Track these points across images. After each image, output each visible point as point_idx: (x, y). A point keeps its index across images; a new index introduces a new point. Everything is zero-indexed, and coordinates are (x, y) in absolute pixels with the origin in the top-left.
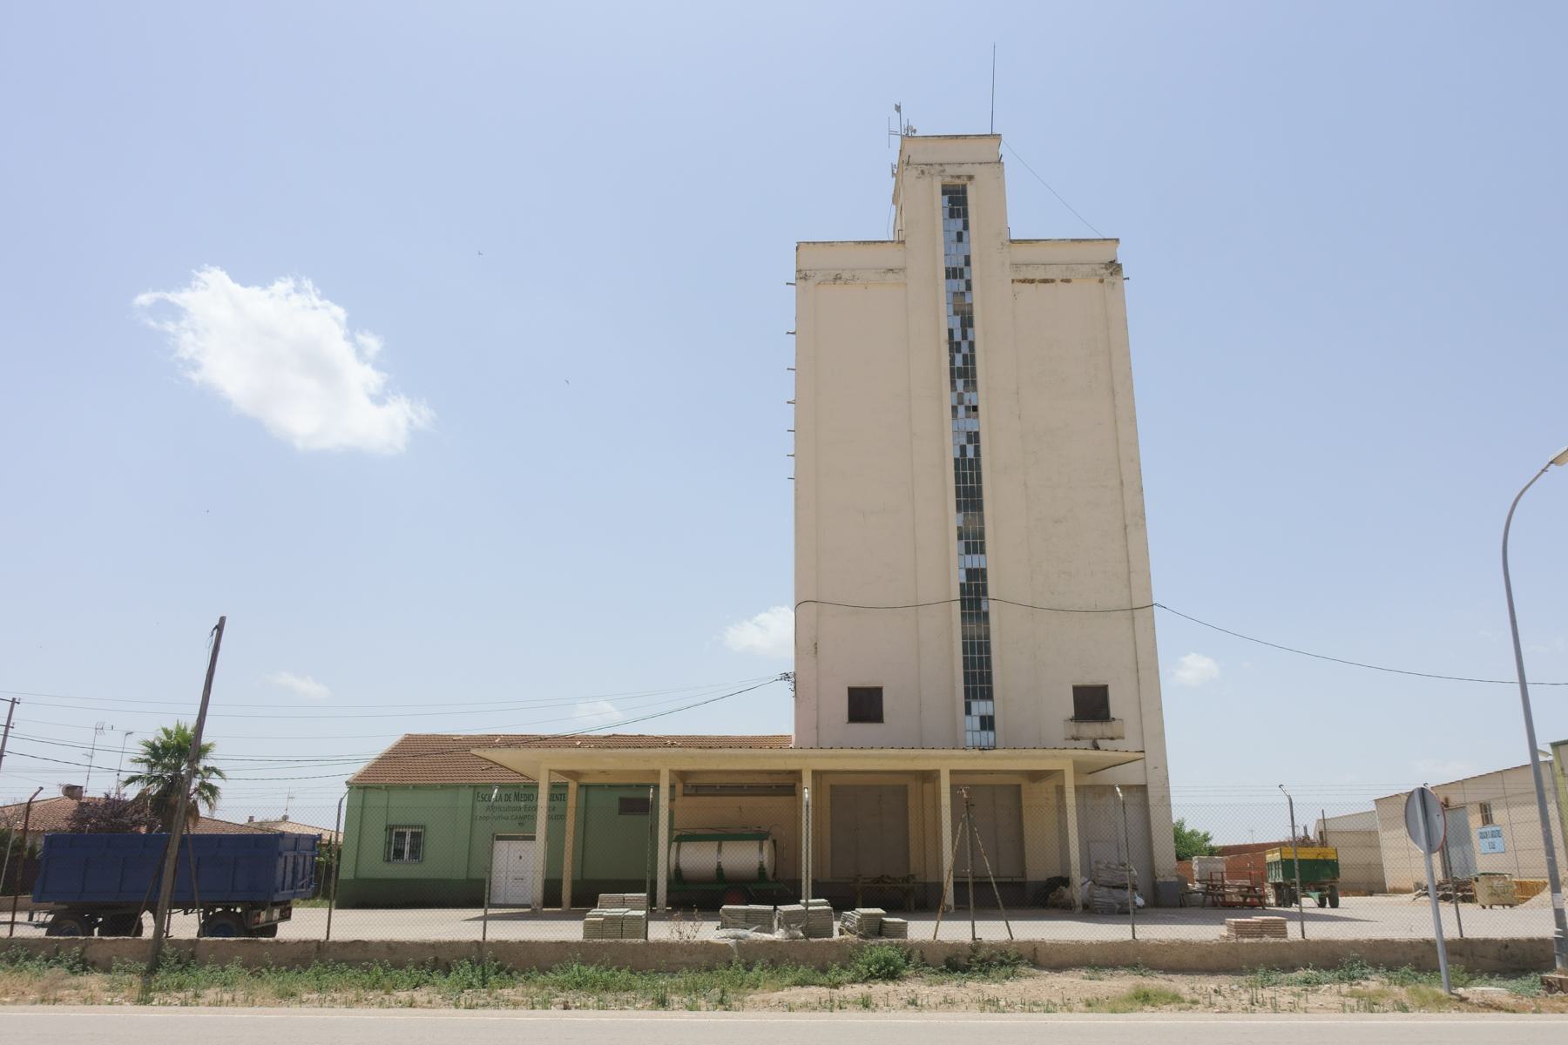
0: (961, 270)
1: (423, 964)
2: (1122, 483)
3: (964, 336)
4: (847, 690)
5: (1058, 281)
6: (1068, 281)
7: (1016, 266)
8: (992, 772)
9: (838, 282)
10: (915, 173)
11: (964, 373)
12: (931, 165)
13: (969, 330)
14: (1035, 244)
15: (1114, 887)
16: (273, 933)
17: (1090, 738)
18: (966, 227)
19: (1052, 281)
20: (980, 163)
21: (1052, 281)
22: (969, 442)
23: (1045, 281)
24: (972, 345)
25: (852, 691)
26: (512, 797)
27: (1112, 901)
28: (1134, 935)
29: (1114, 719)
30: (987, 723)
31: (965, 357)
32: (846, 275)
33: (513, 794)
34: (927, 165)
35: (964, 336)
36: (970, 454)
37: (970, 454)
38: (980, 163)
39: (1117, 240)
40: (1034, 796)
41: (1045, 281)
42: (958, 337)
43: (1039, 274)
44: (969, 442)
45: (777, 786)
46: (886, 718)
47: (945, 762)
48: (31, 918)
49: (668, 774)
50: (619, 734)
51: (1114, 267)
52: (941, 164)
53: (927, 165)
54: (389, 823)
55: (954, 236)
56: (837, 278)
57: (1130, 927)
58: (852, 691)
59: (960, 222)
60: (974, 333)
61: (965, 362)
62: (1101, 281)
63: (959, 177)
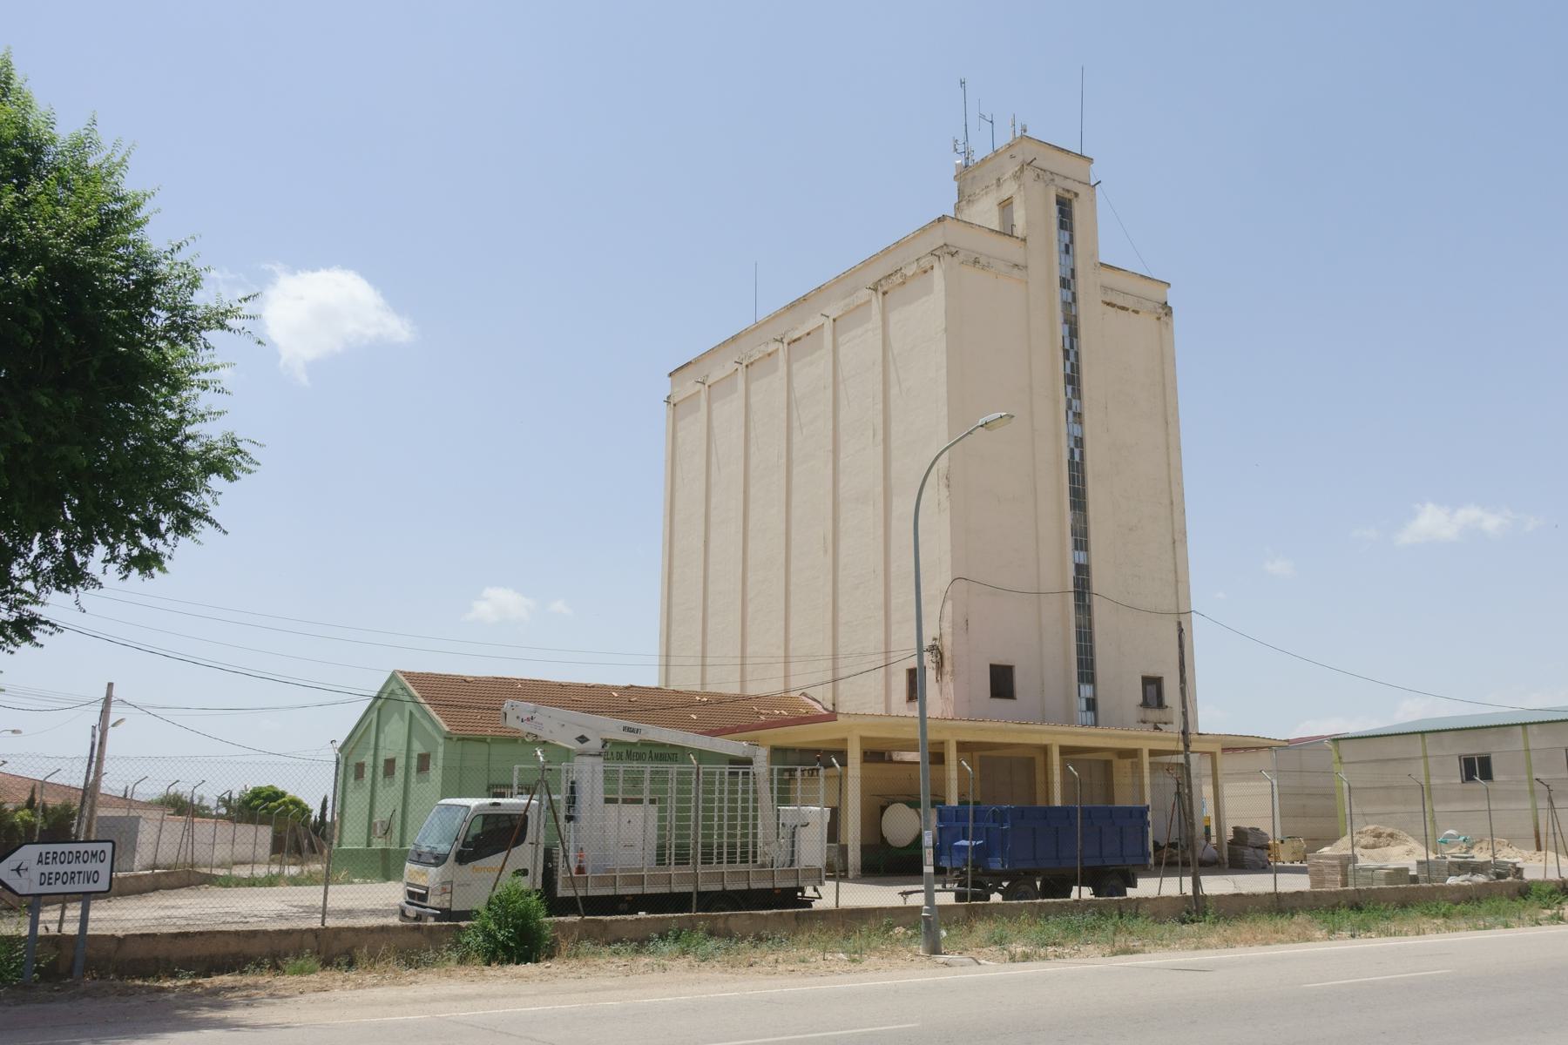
0: (1069, 281)
1: (1471, 898)
2: (1172, 503)
3: (1072, 347)
4: (1160, 675)
5: (1130, 310)
6: (1136, 312)
7: (1105, 288)
8: (1018, 745)
9: (977, 265)
10: (1033, 175)
11: (1073, 379)
12: (1045, 171)
13: (1075, 340)
14: (1117, 272)
15: (1257, 848)
16: (988, 899)
17: (1152, 722)
18: (1072, 241)
19: (1127, 309)
20: (1080, 182)
21: (1127, 309)
22: (1077, 446)
23: (1123, 308)
24: (1077, 354)
25: (992, 666)
26: (624, 755)
27: (1255, 858)
28: (1559, 874)
29: (1167, 707)
30: (1092, 705)
31: (1072, 365)
32: (983, 260)
33: (625, 752)
34: (1041, 170)
35: (1072, 347)
36: (1077, 458)
37: (1077, 458)
38: (1080, 182)
39: (1169, 284)
40: (1122, 767)
41: (1123, 308)
42: (1067, 346)
43: (1120, 302)
44: (1077, 446)
45: (871, 752)
46: (1018, 696)
47: (1057, 736)
48: (944, 886)
49: (955, 744)
50: (637, 685)
51: (1167, 309)
52: (1052, 173)
53: (1041, 170)
54: (491, 782)
55: (1063, 248)
56: (976, 261)
57: (1179, 878)
58: (992, 666)
59: (1067, 234)
60: (1077, 342)
61: (1072, 371)
62: (1159, 319)
63: (1068, 191)
